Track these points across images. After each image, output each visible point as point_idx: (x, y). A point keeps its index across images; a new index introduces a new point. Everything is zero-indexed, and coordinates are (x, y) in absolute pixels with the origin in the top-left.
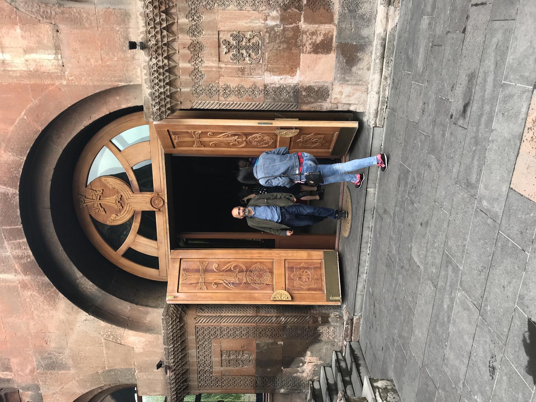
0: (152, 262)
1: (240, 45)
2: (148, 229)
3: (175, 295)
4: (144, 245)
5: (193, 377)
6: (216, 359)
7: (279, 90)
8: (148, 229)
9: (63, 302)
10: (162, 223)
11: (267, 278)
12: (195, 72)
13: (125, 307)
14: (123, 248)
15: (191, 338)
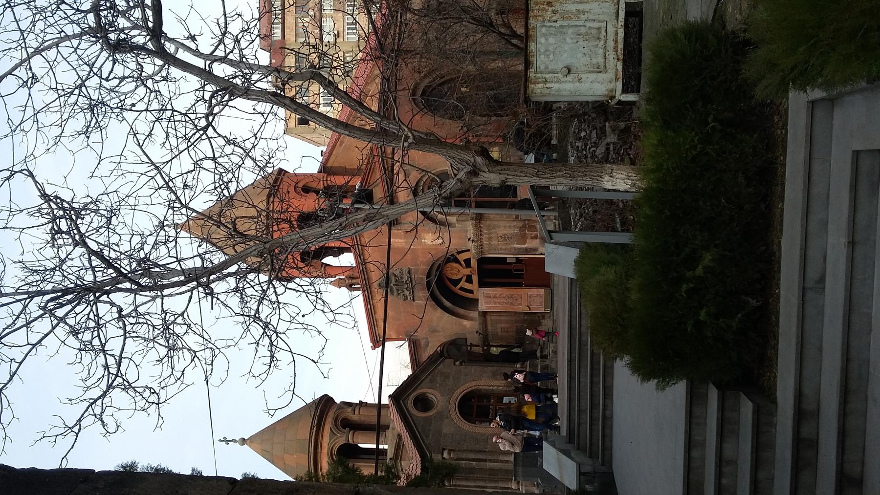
0: (471, 292)
1: (505, 237)
2: (469, 279)
3: (482, 306)
4: (468, 286)
5: (490, 337)
6: (499, 330)
7: (520, 249)
8: (469, 279)
9: (439, 310)
10: (475, 278)
11: (520, 300)
12: (490, 245)
13: (462, 311)
14: (459, 286)
15: (489, 323)
